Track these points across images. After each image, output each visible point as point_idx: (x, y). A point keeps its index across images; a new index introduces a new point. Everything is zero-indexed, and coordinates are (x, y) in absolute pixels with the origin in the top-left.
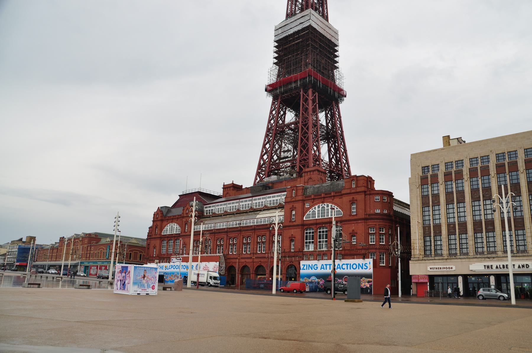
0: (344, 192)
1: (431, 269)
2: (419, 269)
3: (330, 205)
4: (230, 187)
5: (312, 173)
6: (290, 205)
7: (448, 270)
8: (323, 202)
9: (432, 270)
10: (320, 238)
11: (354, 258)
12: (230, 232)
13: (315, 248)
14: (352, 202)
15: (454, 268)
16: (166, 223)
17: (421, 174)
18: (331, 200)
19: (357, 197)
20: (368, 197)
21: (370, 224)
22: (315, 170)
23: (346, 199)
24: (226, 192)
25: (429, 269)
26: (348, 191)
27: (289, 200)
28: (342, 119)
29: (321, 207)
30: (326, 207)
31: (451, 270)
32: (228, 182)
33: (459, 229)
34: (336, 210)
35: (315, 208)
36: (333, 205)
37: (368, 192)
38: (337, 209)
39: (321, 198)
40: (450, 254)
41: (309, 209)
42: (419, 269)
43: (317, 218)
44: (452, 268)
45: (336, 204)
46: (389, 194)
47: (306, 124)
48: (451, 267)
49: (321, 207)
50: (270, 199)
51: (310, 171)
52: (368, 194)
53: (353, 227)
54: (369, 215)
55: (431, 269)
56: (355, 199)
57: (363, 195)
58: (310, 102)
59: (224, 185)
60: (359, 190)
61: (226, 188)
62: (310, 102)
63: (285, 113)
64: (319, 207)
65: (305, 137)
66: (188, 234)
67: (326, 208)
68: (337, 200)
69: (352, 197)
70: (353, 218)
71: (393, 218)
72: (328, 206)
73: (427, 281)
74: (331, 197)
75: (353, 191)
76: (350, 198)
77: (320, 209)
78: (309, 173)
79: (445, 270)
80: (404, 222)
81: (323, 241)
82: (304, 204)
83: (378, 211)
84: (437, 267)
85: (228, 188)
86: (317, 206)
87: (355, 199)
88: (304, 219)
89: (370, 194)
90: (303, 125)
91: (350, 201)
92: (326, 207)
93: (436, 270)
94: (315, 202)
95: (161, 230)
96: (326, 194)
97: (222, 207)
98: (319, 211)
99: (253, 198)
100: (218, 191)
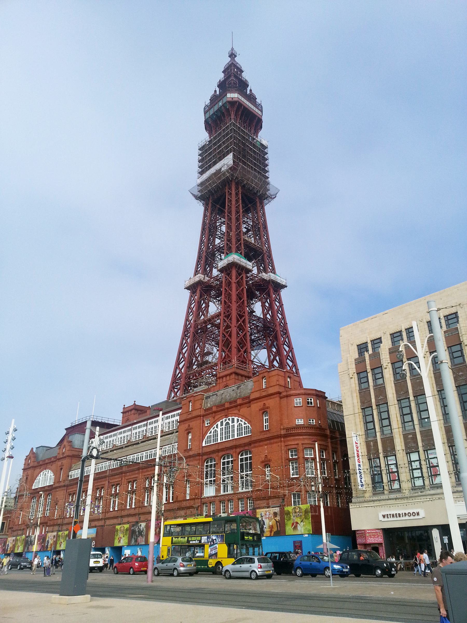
0: (252, 397)
1: (384, 516)
2: (367, 518)
3: (236, 419)
4: (131, 410)
5: (228, 378)
6: (186, 426)
7: (412, 517)
8: (226, 416)
9: (386, 519)
10: (224, 474)
13: (218, 490)
14: (264, 411)
15: (422, 514)
16: (39, 470)
17: (357, 356)
18: (236, 412)
20: (284, 400)
21: (290, 443)
22: (231, 374)
23: (256, 406)
25: (381, 518)
26: (257, 395)
27: (185, 417)
28: (284, 306)
29: (224, 423)
30: (230, 422)
31: (416, 517)
32: (129, 404)
33: (423, 441)
35: (217, 427)
36: (240, 419)
37: (284, 394)
38: (245, 424)
39: (224, 410)
40: (414, 488)
41: (209, 428)
42: (367, 518)
43: (219, 441)
44: (418, 514)
45: (243, 417)
46: (320, 395)
47: (229, 315)
48: (416, 511)
49: (224, 423)
50: (169, 420)
51: (226, 376)
52: (284, 397)
54: (288, 429)
55: (384, 516)
56: (267, 405)
57: (278, 399)
58: (234, 286)
59: (124, 408)
60: (271, 391)
62: (234, 286)
63: (207, 306)
64: (222, 425)
65: (227, 332)
67: (231, 424)
68: (244, 410)
69: (263, 403)
70: (265, 436)
71: (328, 432)
72: (233, 420)
73: (380, 539)
74: (236, 406)
75: (264, 394)
77: (224, 426)
78: (224, 378)
79: (407, 517)
80: (331, 435)
82: (203, 422)
83: (300, 422)
84: (394, 512)
85: (128, 411)
86: (219, 423)
87: (267, 405)
89: (287, 396)
90: (225, 316)
91: (260, 410)
92: (230, 422)
93: (392, 519)
94: (216, 418)
96: (231, 403)
98: (221, 429)
99: (149, 421)
100: (116, 418)
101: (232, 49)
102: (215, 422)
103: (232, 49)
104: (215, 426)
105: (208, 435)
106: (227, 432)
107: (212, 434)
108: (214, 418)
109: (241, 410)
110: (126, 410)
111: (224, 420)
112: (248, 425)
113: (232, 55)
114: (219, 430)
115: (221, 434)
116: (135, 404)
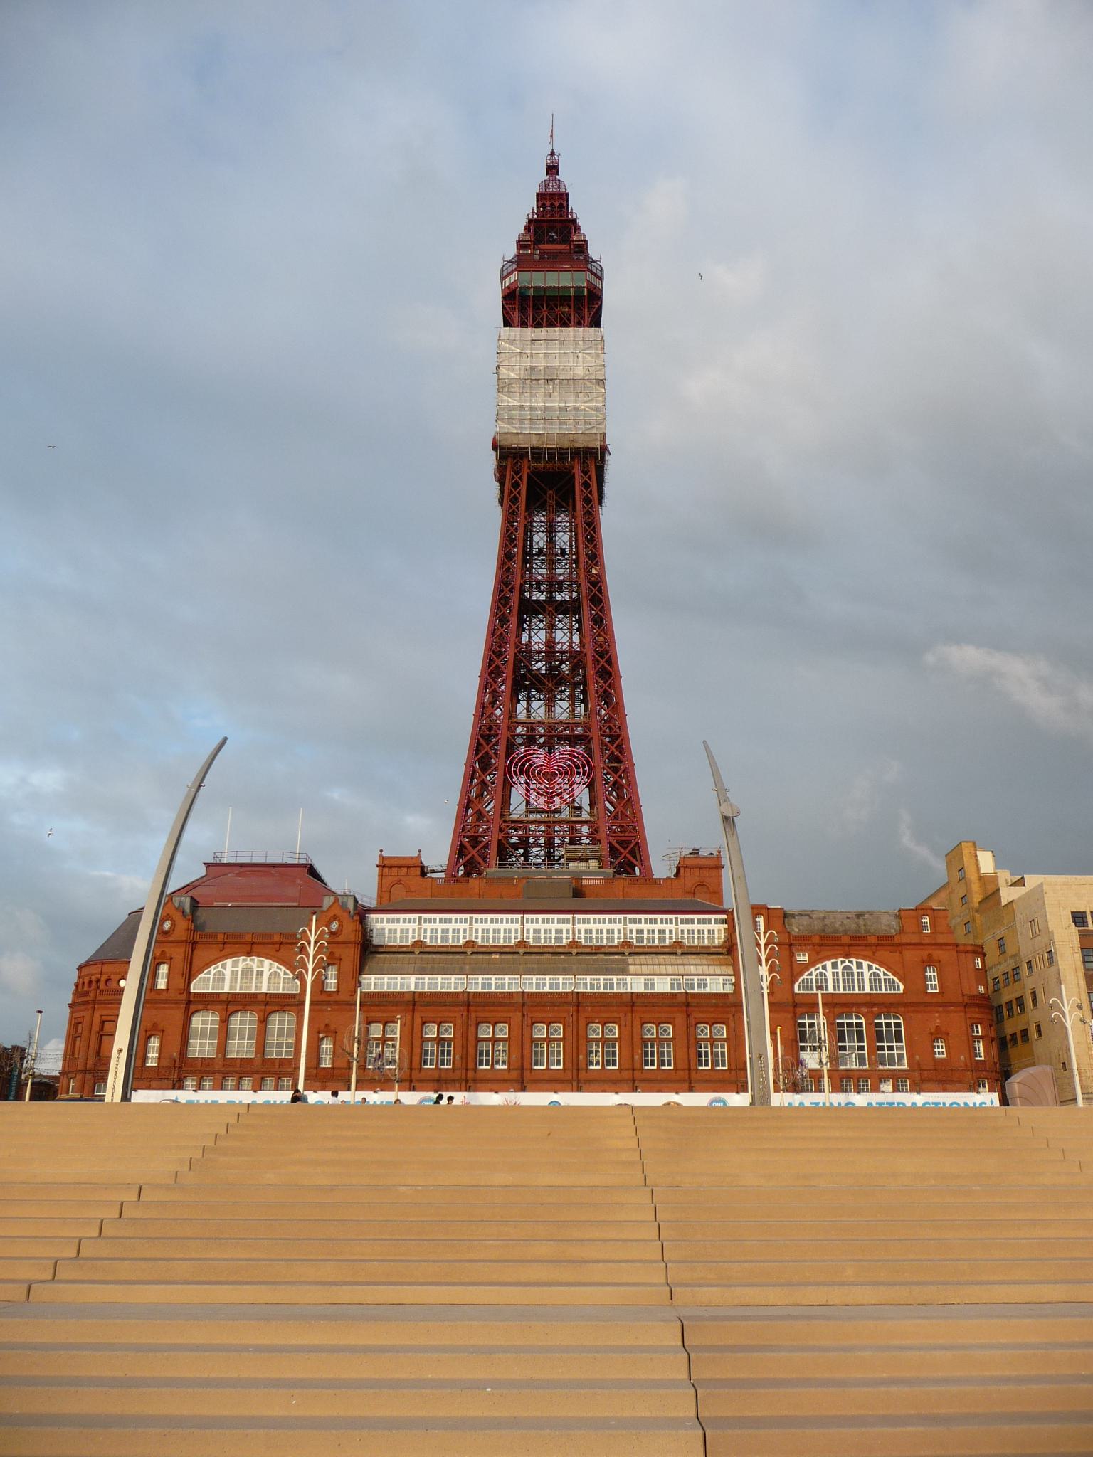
3: (865, 964)
4: (408, 867)
8: (847, 956)
11: (945, 1090)
12: (478, 1004)
14: (929, 962)
18: (870, 954)
19: (937, 954)
23: (910, 955)
24: (390, 880)
29: (840, 967)
30: (854, 967)
34: (882, 977)
35: (824, 968)
36: (874, 966)
45: (882, 964)
49: (840, 967)
53: (936, 1020)
57: (954, 953)
59: (382, 858)
61: (386, 865)
64: (835, 966)
66: (348, 999)
67: (855, 970)
68: (883, 954)
72: (859, 966)
74: (870, 945)
75: (927, 940)
76: (924, 953)
77: (840, 970)
81: (852, 1048)
82: (792, 955)
86: (828, 964)
88: (796, 991)
92: (854, 967)
95: (190, 976)
97: (451, 927)
101: (552, 153)
102: (821, 960)
103: (552, 153)
104: (820, 966)
105: (805, 976)
106: (848, 982)
107: (814, 977)
108: (818, 953)
109: (878, 953)
110: (386, 862)
111: (839, 961)
112: (891, 977)
113: (552, 169)
114: (829, 973)
115: (835, 981)
116: (419, 856)
